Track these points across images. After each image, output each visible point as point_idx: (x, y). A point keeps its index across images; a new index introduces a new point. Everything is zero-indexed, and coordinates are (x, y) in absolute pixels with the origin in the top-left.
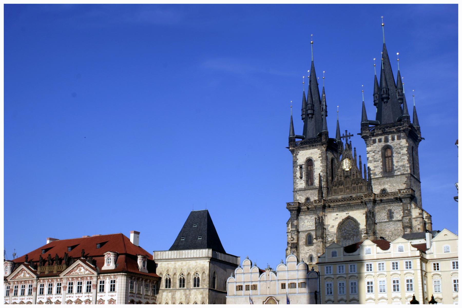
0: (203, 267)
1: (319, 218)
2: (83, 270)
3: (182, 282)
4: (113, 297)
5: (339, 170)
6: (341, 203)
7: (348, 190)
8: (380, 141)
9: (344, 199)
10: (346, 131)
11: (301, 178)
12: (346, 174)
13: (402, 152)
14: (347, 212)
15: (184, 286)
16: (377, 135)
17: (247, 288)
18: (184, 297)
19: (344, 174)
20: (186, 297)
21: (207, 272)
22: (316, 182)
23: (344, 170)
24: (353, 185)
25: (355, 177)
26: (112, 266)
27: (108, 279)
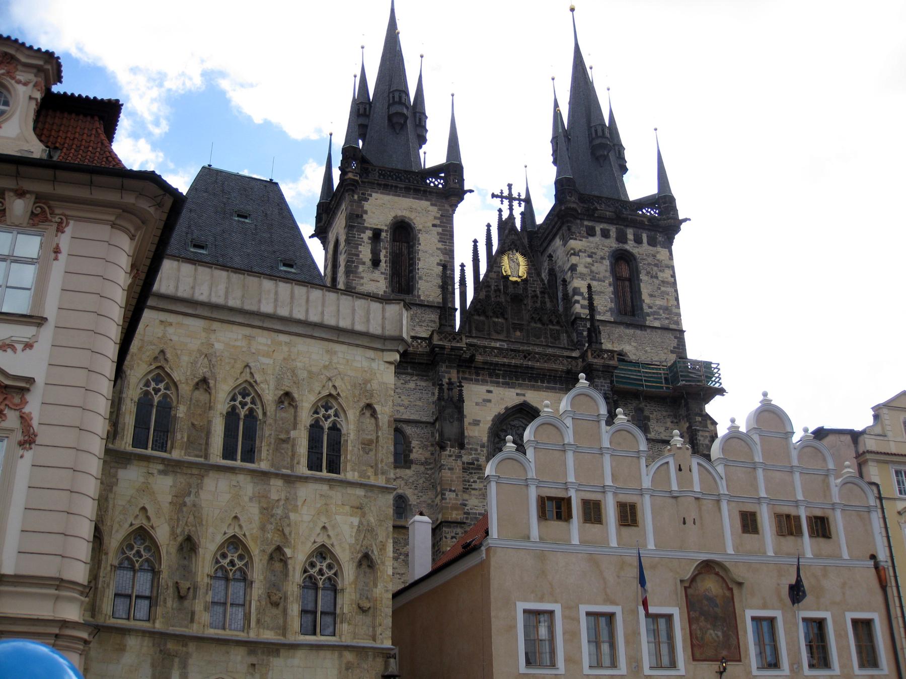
0: (367, 382)
1: (450, 383)
3: (243, 435)
6: (505, 360)
7: (518, 333)
8: (605, 234)
10: (510, 186)
12: (511, 290)
13: (660, 275)
14: (519, 391)
15: (250, 455)
16: (601, 219)
17: (593, 512)
18: (254, 510)
19: (506, 287)
20: (267, 511)
24: (533, 325)
25: (538, 305)
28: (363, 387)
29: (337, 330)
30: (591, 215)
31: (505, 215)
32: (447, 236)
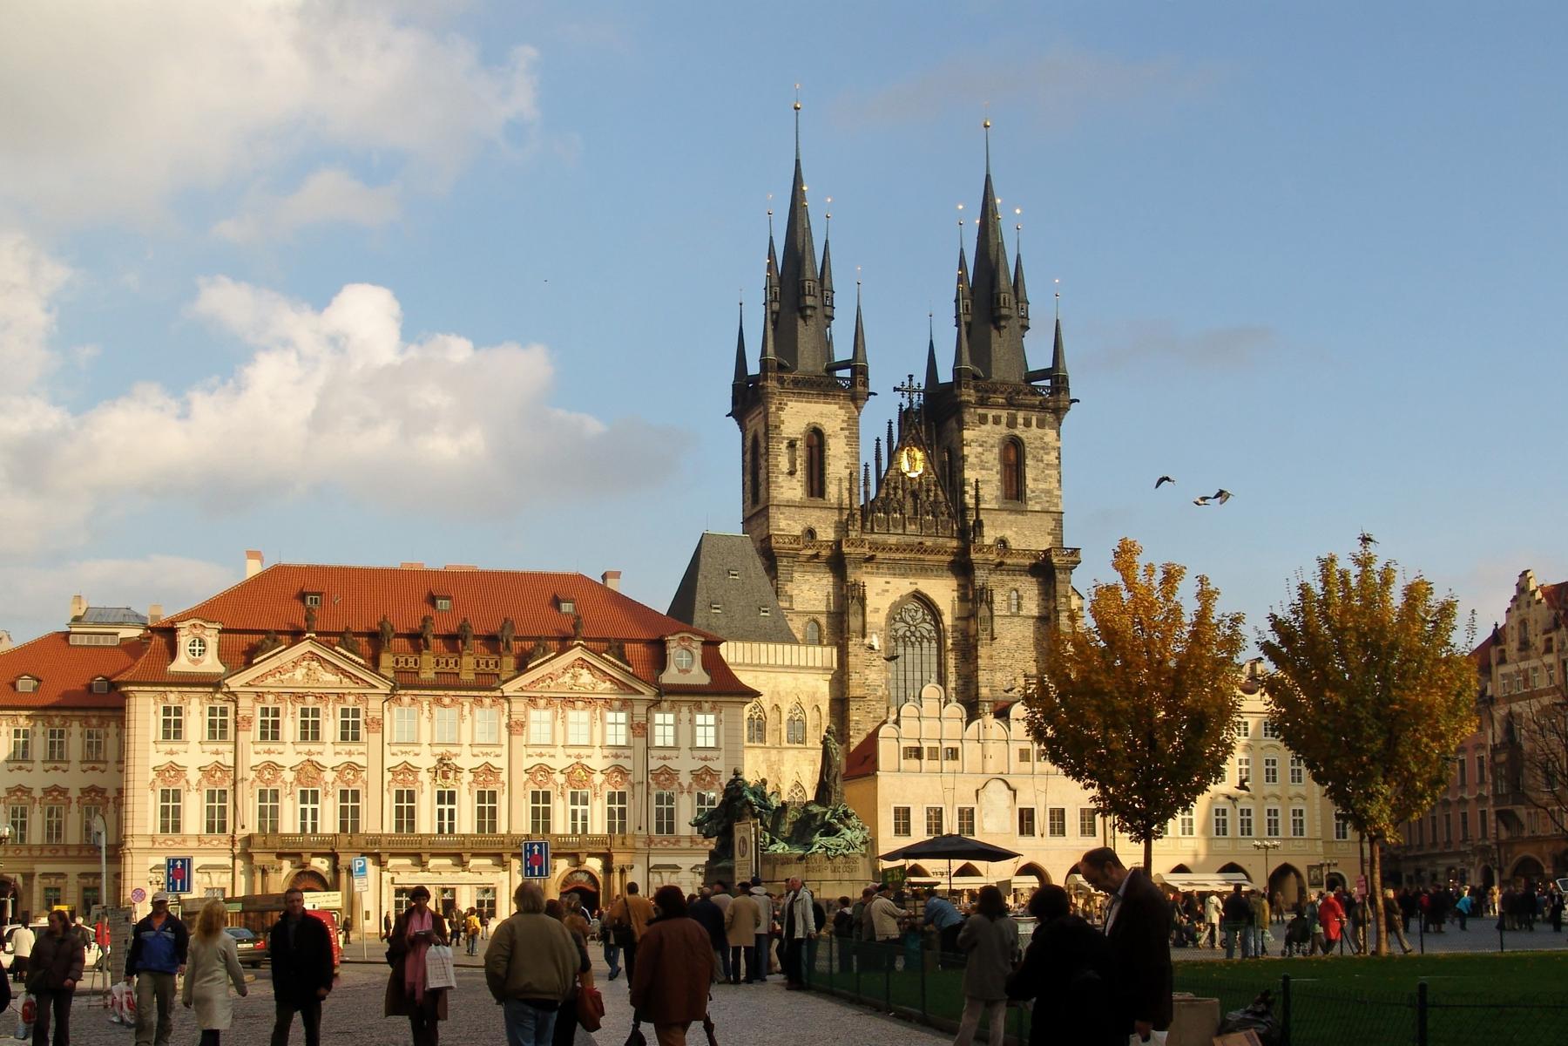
2: (586, 677)
4: (708, 763)
5: (892, 472)
8: (997, 421)
9: (909, 548)
10: (911, 377)
11: (792, 473)
15: (762, 739)
17: (934, 754)
18: (764, 767)
20: (770, 767)
21: (825, 708)
22: (832, 490)
23: (903, 474)
26: (698, 676)
27: (685, 710)
28: (813, 696)
29: (799, 667)
30: (982, 403)
31: (906, 405)
32: (853, 438)
